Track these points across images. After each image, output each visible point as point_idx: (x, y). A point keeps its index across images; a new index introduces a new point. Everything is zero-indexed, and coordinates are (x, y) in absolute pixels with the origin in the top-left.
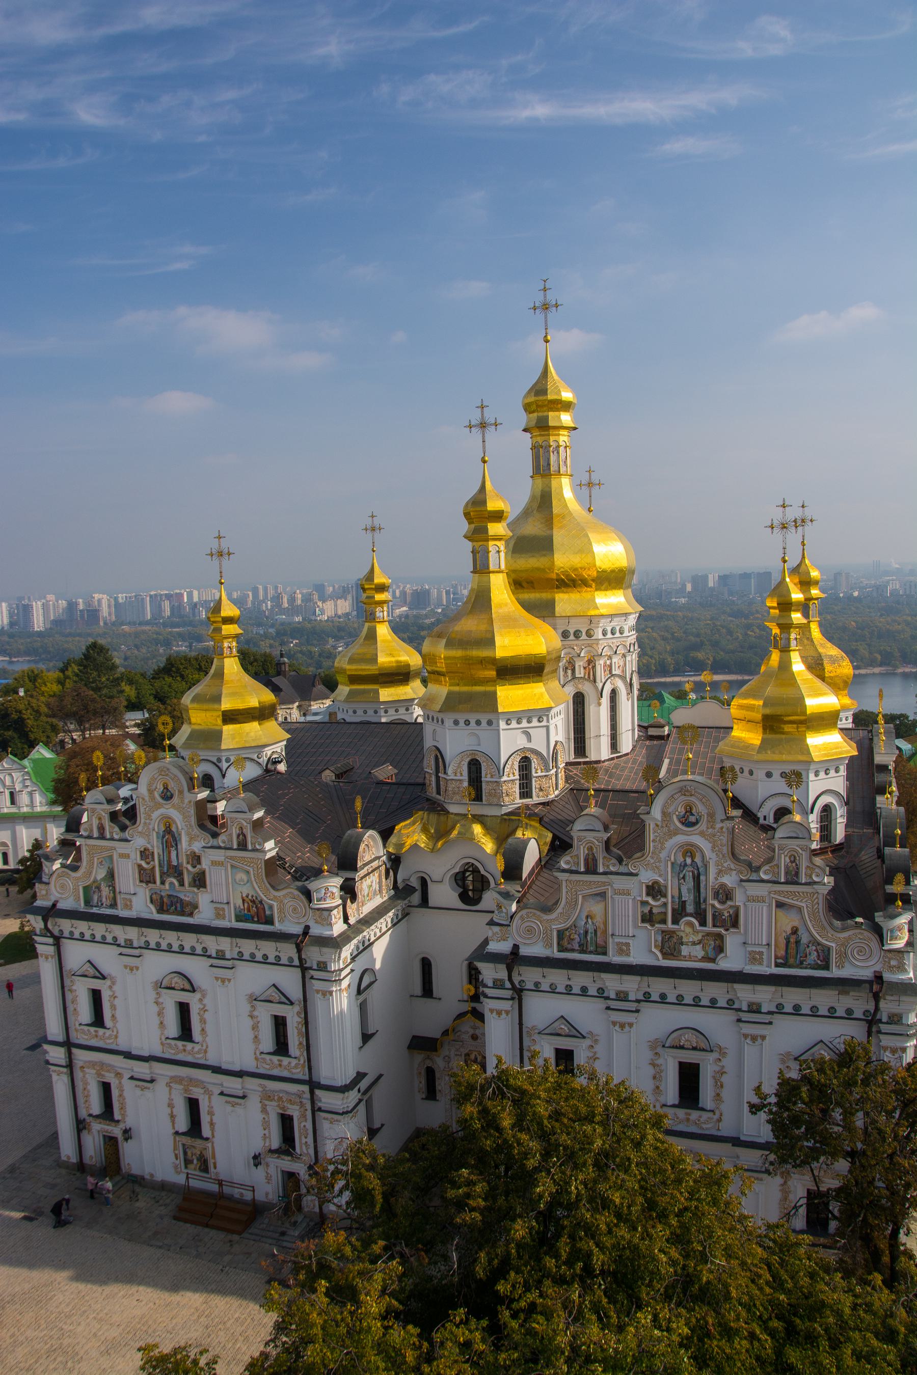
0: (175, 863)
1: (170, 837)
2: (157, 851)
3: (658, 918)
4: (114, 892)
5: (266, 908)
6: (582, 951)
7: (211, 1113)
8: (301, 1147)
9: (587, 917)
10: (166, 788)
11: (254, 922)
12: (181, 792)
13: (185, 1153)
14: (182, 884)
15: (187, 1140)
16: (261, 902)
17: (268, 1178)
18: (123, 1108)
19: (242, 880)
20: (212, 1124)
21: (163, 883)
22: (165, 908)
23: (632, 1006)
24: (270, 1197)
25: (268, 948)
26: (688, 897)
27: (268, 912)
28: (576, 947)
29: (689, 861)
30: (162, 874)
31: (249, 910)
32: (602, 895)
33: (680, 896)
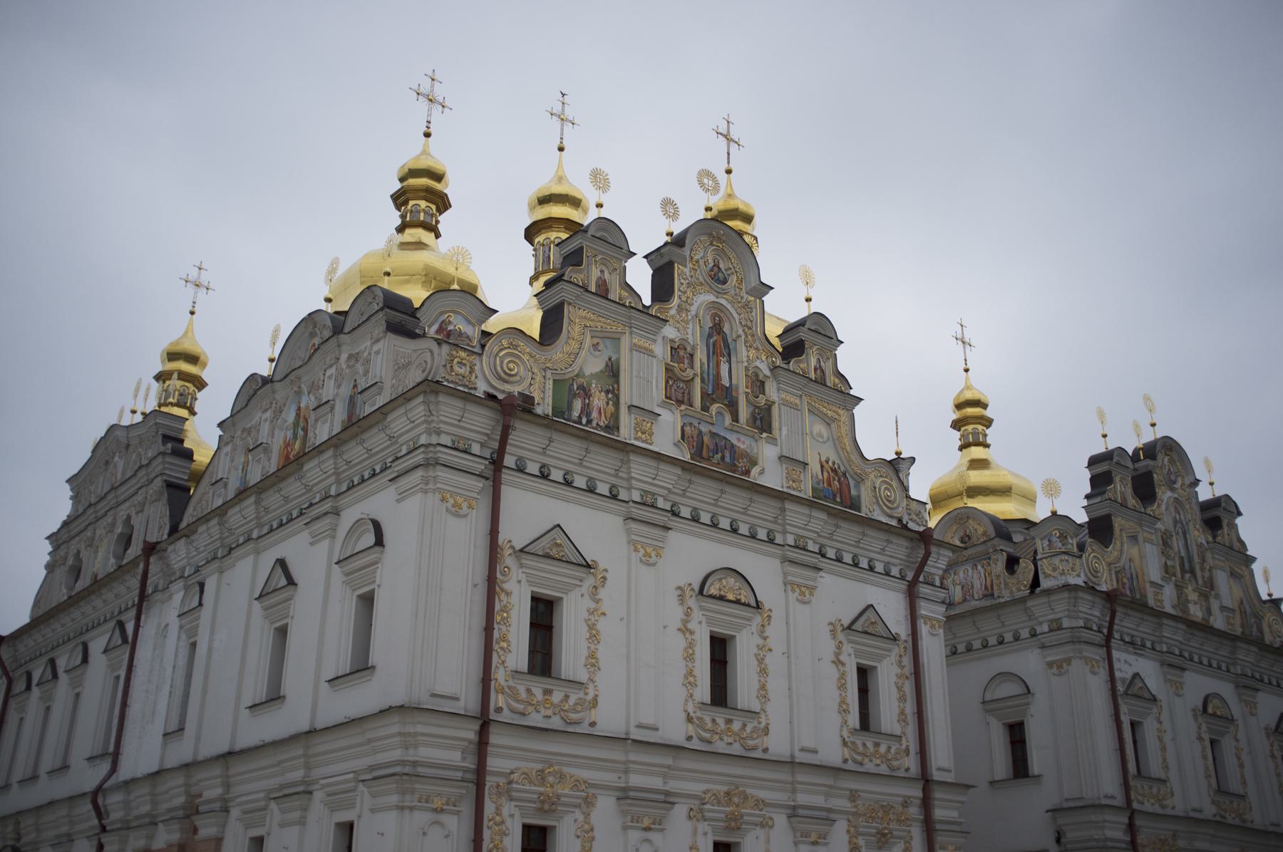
2: (701, 356)
4: (617, 405)
5: (852, 483)
9: (1130, 560)
10: (716, 265)
11: (834, 501)
16: (844, 474)
19: (820, 435)
21: (705, 408)
22: (705, 453)
26: (1183, 554)
27: (853, 492)
29: (1178, 517)
30: (705, 395)
33: (1179, 552)
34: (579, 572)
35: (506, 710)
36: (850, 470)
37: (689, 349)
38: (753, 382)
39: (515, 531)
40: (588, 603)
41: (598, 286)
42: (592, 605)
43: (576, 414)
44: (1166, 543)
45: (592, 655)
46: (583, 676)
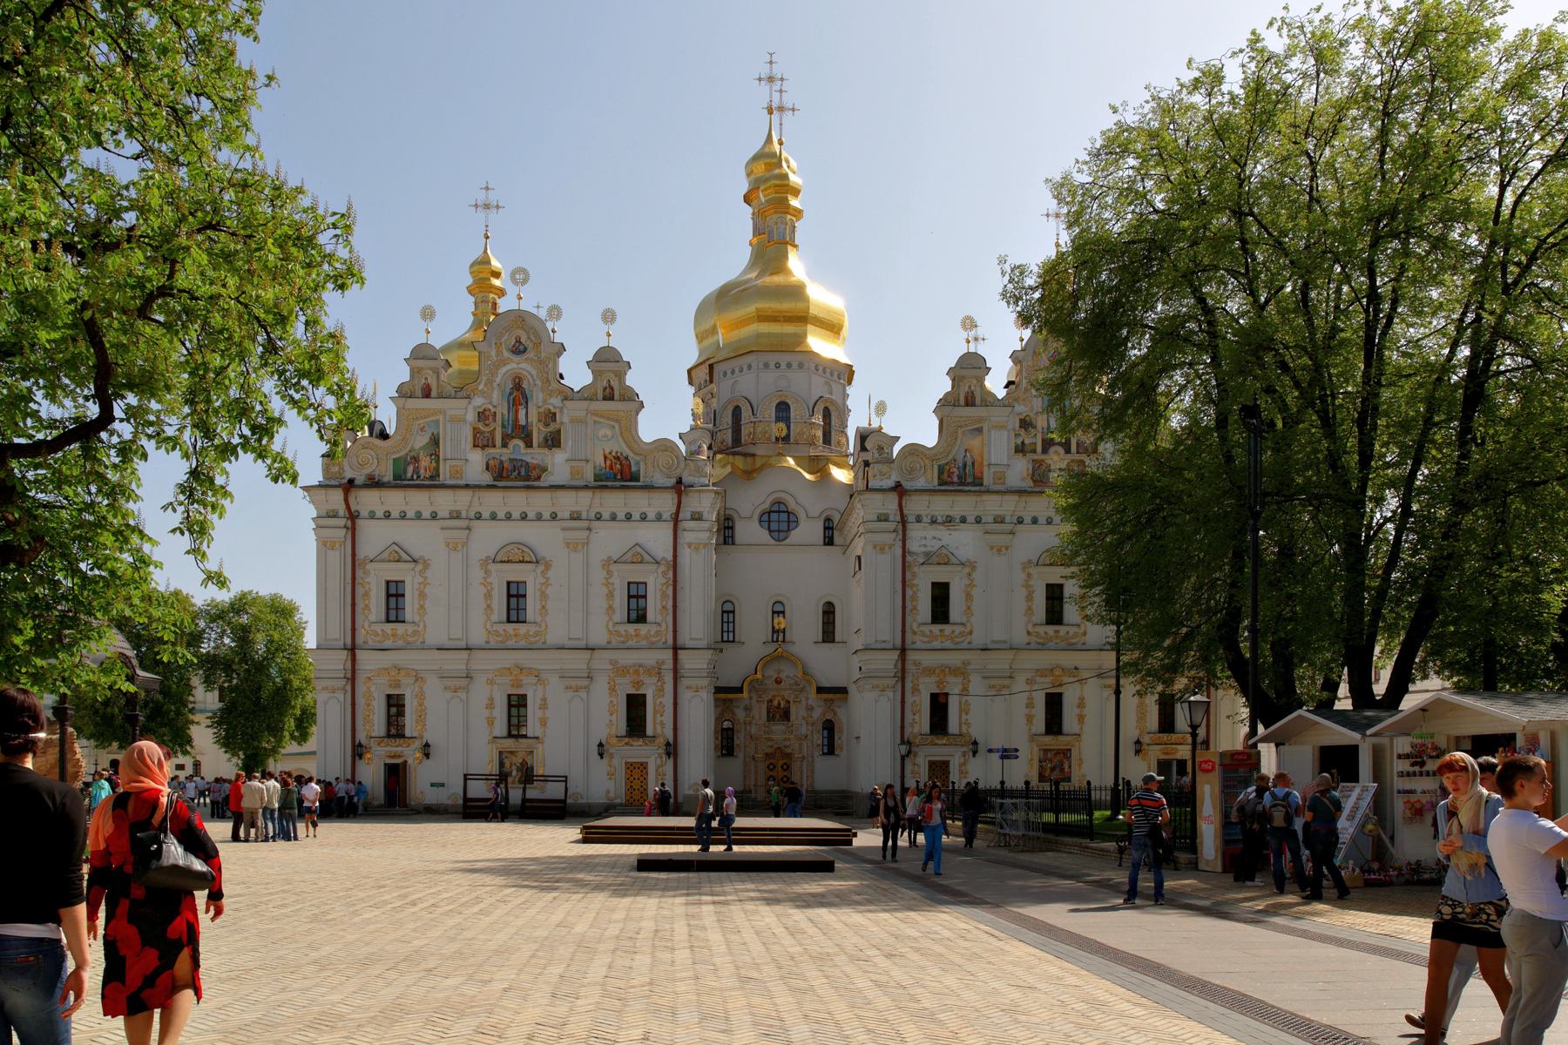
0: (522, 422)
1: (518, 394)
2: (502, 410)
3: (1029, 448)
4: (438, 462)
6: (962, 484)
7: (544, 705)
8: (655, 728)
10: (519, 341)
11: (615, 479)
12: (537, 345)
13: (502, 764)
14: (529, 444)
15: (509, 744)
16: (627, 458)
17: (611, 775)
18: (421, 718)
19: (606, 436)
20: (544, 723)
23: (1010, 527)
24: (612, 795)
25: (637, 502)
27: (634, 469)
28: (955, 479)
31: (611, 468)
32: (980, 430)
34: (412, 565)
35: (370, 642)
36: (631, 455)
37: (493, 410)
38: (546, 415)
39: (367, 549)
40: (419, 579)
41: (423, 389)
42: (421, 580)
43: (409, 475)
44: (1026, 424)
45: (422, 607)
46: (417, 619)
